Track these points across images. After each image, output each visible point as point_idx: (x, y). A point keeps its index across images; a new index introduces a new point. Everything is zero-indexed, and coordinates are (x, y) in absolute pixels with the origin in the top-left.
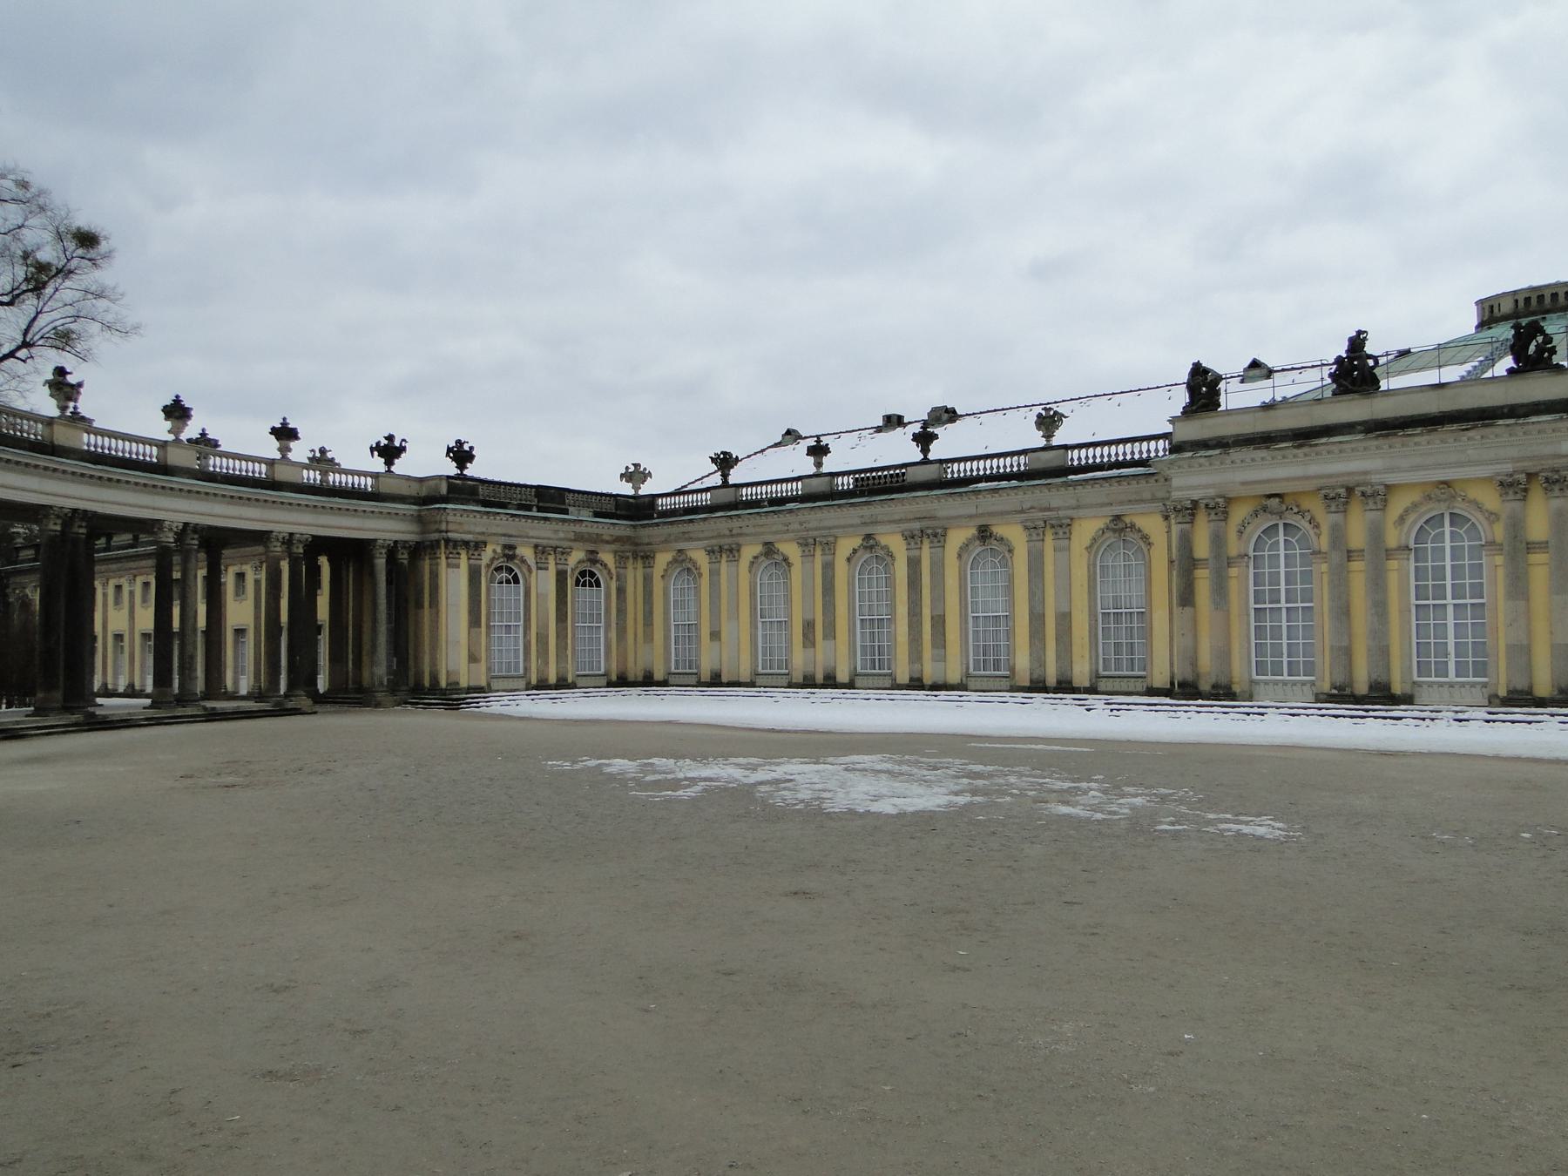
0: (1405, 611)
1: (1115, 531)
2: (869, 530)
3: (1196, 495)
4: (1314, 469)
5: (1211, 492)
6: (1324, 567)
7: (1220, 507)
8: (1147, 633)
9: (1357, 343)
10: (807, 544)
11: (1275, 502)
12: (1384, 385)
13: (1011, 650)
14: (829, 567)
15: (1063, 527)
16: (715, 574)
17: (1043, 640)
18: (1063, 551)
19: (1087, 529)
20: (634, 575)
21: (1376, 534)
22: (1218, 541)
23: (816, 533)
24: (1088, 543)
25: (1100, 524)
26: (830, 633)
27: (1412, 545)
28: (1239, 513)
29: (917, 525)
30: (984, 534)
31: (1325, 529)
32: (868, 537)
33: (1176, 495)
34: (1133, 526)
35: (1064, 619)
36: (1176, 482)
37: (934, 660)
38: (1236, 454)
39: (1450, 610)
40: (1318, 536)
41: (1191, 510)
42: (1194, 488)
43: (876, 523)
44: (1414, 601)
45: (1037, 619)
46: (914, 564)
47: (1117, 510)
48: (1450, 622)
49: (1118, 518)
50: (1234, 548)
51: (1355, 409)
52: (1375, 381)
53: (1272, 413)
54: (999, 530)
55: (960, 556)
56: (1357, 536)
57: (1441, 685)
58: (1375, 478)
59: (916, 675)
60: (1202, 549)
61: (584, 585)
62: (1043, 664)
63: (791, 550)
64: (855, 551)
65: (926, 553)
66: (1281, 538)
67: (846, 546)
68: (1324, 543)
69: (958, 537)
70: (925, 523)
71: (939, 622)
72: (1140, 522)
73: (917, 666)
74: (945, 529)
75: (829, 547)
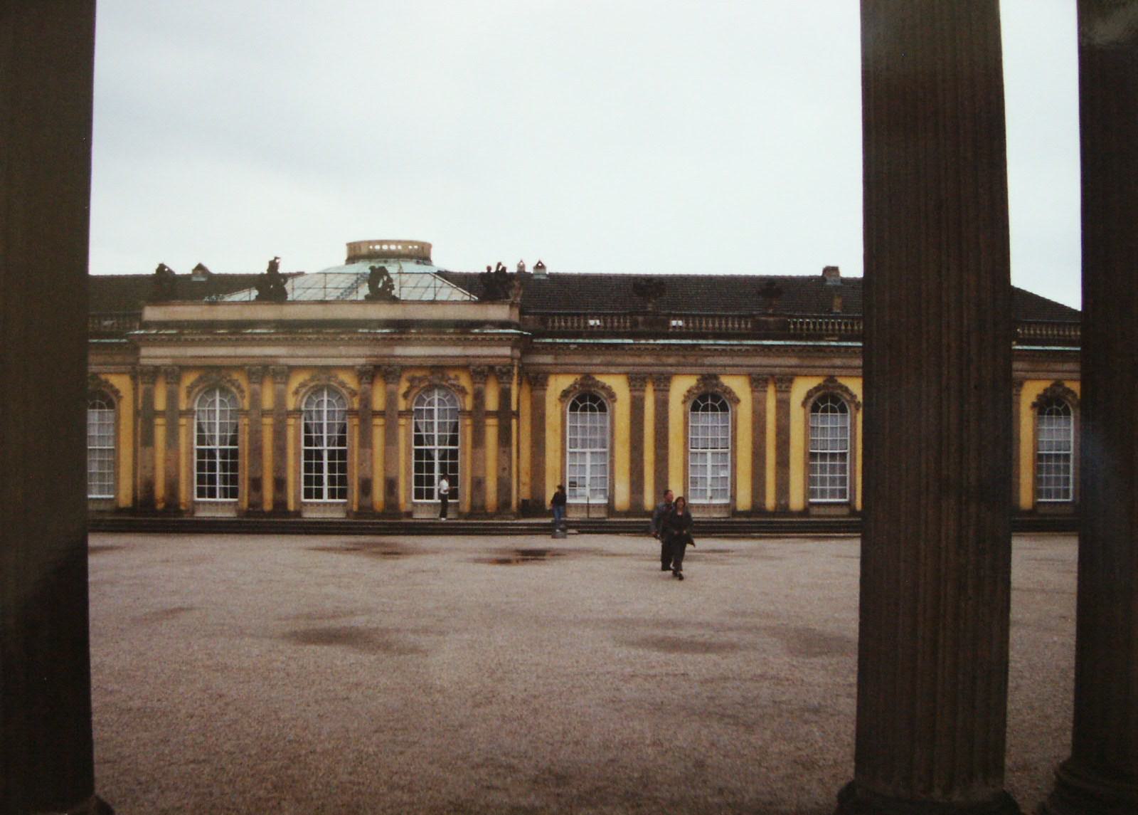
0: (297, 454)
3: (158, 362)
5: (168, 361)
6: (246, 421)
7: (173, 374)
8: (115, 465)
9: (273, 265)
12: (290, 298)
21: (280, 399)
22: (172, 398)
27: (303, 408)
28: (189, 379)
31: (247, 394)
33: (143, 361)
36: (144, 351)
40: (243, 398)
41: (154, 373)
42: (156, 357)
44: (303, 447)
52: (285, 294)
56: (268, 401)
58: (282, 361)
60: (160, 403)
68: (246, 404)
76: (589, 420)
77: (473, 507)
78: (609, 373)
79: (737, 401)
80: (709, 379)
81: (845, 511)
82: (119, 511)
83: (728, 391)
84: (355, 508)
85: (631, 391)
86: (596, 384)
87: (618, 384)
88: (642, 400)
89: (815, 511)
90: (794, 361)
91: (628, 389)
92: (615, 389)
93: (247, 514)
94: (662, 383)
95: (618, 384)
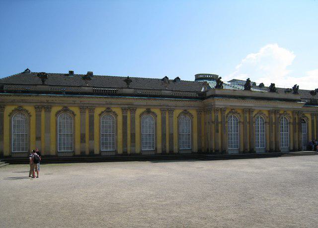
1: (107, 111)
2: (109, 106)
3: (221, 107)
4: (243, 105)
5: (224, 107)
7: (222, 110)
10: (82, 109)
11: (233, 111)
13: (156, 144)
14: (92, 118)
16: (38, 117)
17: (170, 141)
18: (171, 117)
19: (177, 112)
22: (223, 118)
23: (88, 105)
26: (92, 138)
29: (127, 106)
30: (148, 111)
32: (108, 108)
33: (216, 106)
35: (171, 135)
38: (231, 99)
41: (217, 110)
43: (111, 104)
45: (164, 135)
46: (125, 118)
47: (186, 108)
49: (185, 110)
54: (152, 110)
58: (253, 108)
62: (165, 147)
63: (76, 110)
64: (102, 112)
65: (129, 115)
67: (98, 111)
69: (139, 111)
71: (133, 136)
72: (191, 112)
73: (126, 148)
74: (136, 108)
75: (92, 109)
77: (270, 149)
82: (193, 153)
84: (268, 150)
88: (126, 117)
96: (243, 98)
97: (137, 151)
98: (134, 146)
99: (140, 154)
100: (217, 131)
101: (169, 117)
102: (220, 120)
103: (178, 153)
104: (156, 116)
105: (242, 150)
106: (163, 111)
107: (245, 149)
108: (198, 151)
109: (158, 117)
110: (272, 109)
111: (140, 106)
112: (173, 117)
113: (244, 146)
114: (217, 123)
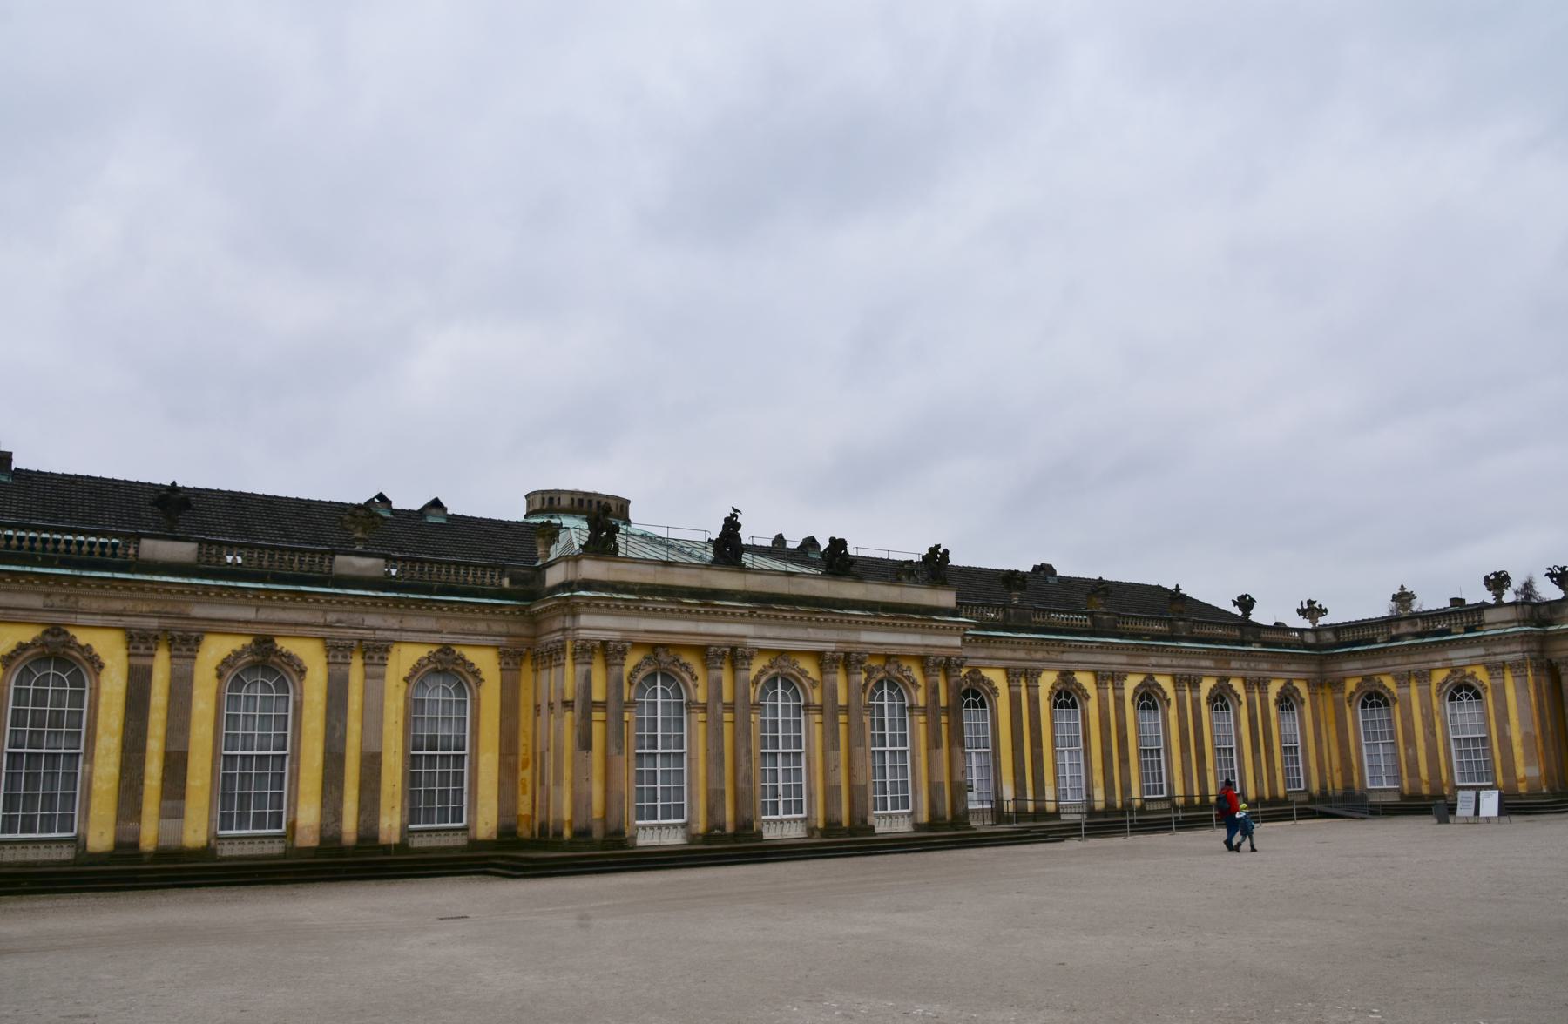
3: (604, 636)
4: (704, 627)
5: (617, 636)
7: (610, 652)
15: (376, 652)
18: (375, 675)
19: (405, 658)
20: (1327, 701)
24: (407, 673)
25: (423, 652)
28: (633, 659)
29: (153, 623)
30: (264, 645)
31: (701, 681)
33: (583, 634)
34: (461, 658)
35: (372, 763)
37: (164, 814)
39: (780, 757)
46: (138, 683)
48: (780, 768)
49: (446, 649)
50: (628, 693)
51: (726, 580)
53: (670, 569)
55: (220, 675)
57: (775, 821)
58: (750, 642)
59: (129, 839)
61: (1372, 706)
62: (338, 817)
65: (161, 665)
66: (659, 686)
69: (216, 649)
70: (167, 623)
71: (176, 764)
72: (471, 655)
76: (1379, 715)
77: (828, 822)
78: (991, 668)
79: (1088, 698)
80: (1066, 675)
81: (1166, 805)
82: (475, 844)
83: (1079, 686)
84: (820, 825)
85: (129, 655)
86: (983, 679)
87: (997, 677)
88: (148, 672)
89: (1149, 807)
90: (1124, 659)
91: (324, 660)
92: (307, 663)
93: (708, 837)
94: (1032, 676)
95: (997, 677)
96: (706, 596)
97: (195, 830)
98: (179, 814)
99: (207, 852)
100: (585, 743)
101: (367, 676)
102: (598, 695)
103: (403, 847)
104: (302, 672)
105: (700, 827)
106: (337, 652)
107: (715, 824)
108: (500, 834)
109: (308, 674)
110: (832, 647)
111: (223, 627)
112: (382, 677)
113: (710, 812)
114: (589, 706)
